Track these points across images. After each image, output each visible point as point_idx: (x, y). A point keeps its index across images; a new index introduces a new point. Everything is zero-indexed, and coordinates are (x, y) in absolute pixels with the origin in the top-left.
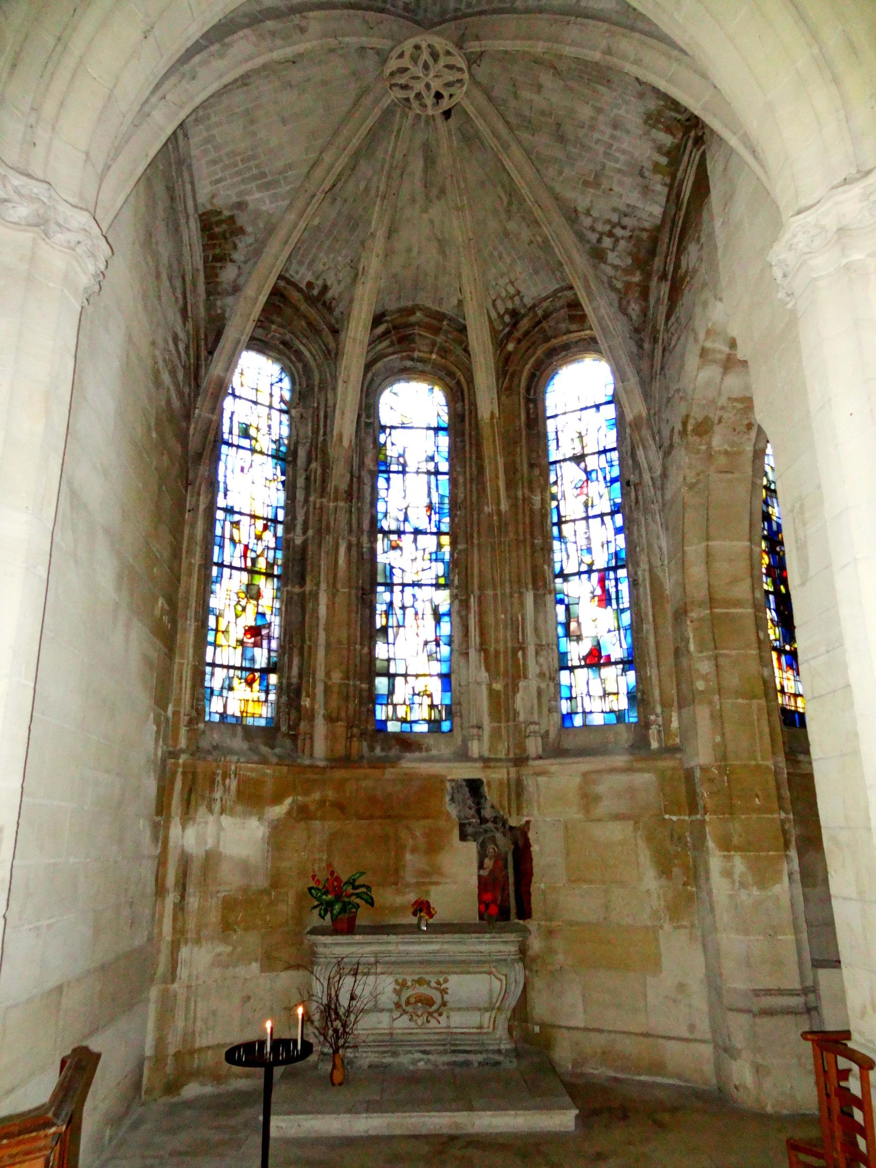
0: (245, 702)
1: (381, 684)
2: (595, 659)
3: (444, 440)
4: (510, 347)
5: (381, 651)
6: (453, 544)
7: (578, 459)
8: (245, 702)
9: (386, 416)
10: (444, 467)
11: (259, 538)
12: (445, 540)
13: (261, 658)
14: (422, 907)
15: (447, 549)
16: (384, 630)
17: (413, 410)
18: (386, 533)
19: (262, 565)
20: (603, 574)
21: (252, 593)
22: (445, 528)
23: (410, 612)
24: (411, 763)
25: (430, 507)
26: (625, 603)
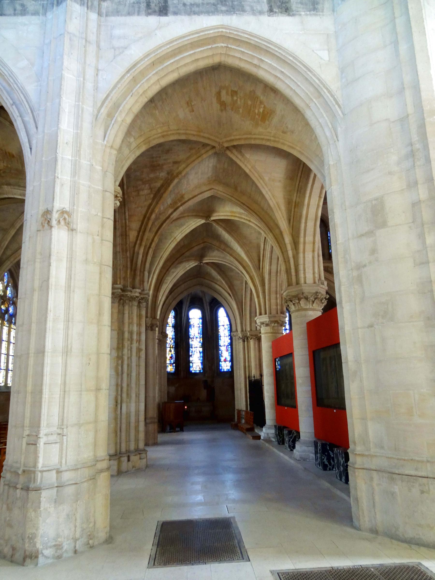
0: (170, 369)
1: (191, 364)
2: (225, 360)
3: (201, 321)
4: (212, 305)
5: (191, 359)
6: (203, 340)
7: (223, 326)
8: (170, 369)
9: (190, 317)
10: (201, 326)
11: (171, 341)
12: (201, 339)
13: (172, 361)
14: (198, 399)
15: (201, 341)
16: (191, 355)
17: (195, 316)
18: (191, 338)
19: (172, 346)
20: (227, 346)
21: (170, 351)
22: (201, 337)
23: (195, 352)
24: (196, 377)
25: (199, 333)
26: (230, 351)
